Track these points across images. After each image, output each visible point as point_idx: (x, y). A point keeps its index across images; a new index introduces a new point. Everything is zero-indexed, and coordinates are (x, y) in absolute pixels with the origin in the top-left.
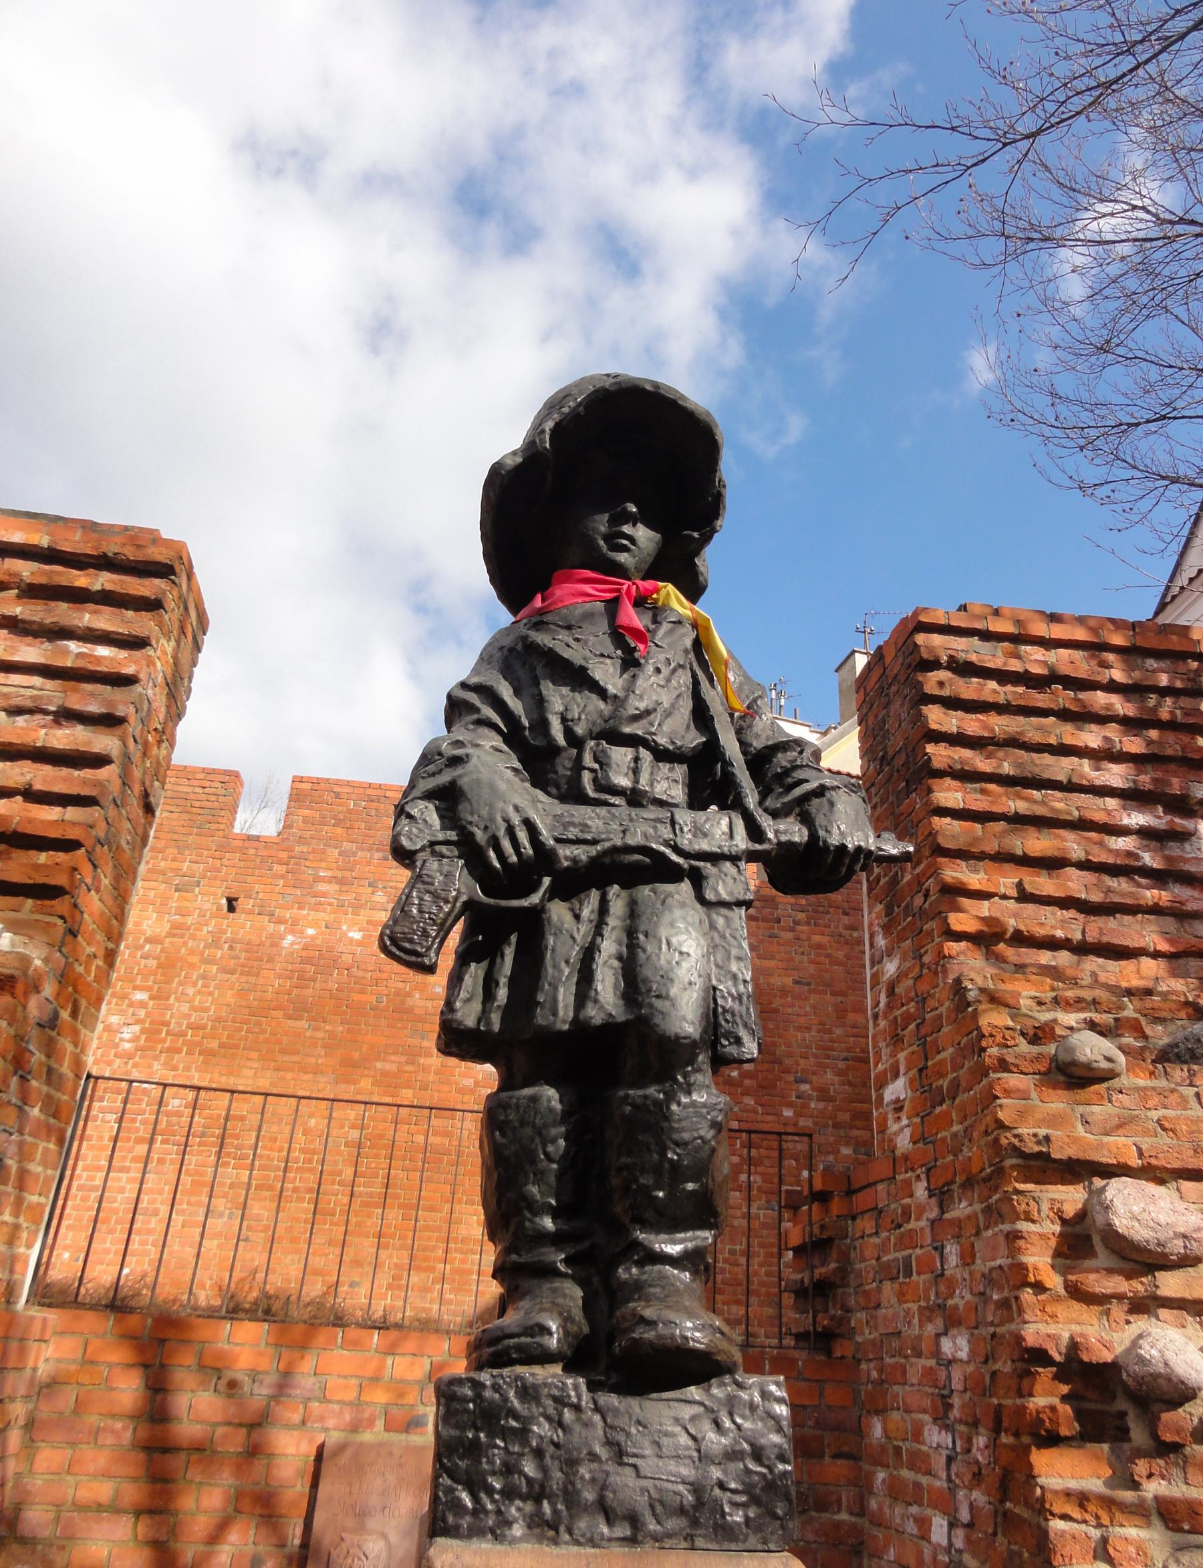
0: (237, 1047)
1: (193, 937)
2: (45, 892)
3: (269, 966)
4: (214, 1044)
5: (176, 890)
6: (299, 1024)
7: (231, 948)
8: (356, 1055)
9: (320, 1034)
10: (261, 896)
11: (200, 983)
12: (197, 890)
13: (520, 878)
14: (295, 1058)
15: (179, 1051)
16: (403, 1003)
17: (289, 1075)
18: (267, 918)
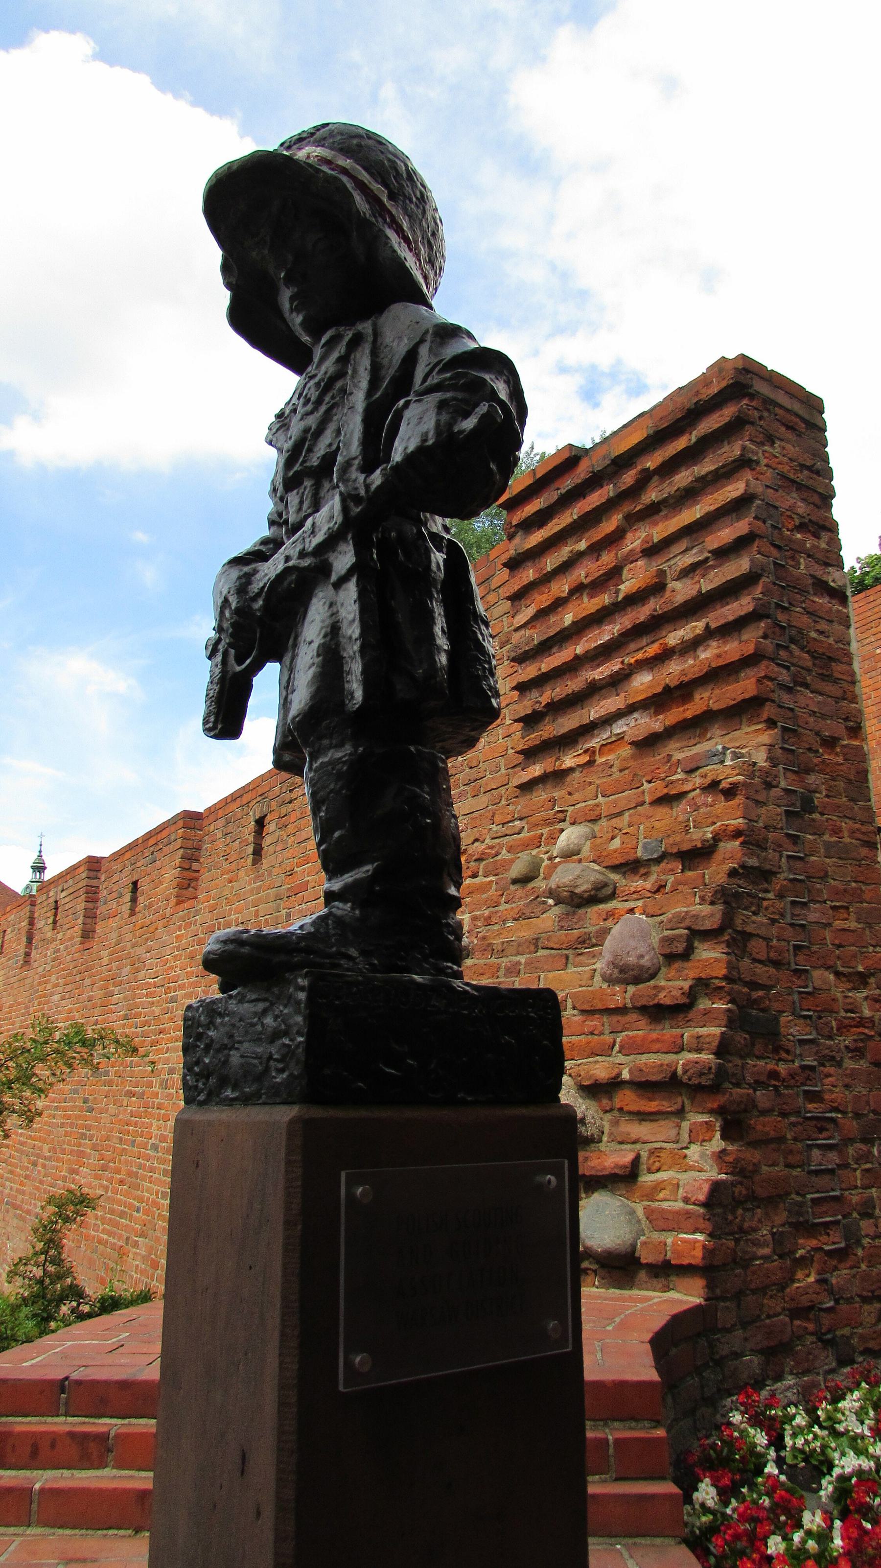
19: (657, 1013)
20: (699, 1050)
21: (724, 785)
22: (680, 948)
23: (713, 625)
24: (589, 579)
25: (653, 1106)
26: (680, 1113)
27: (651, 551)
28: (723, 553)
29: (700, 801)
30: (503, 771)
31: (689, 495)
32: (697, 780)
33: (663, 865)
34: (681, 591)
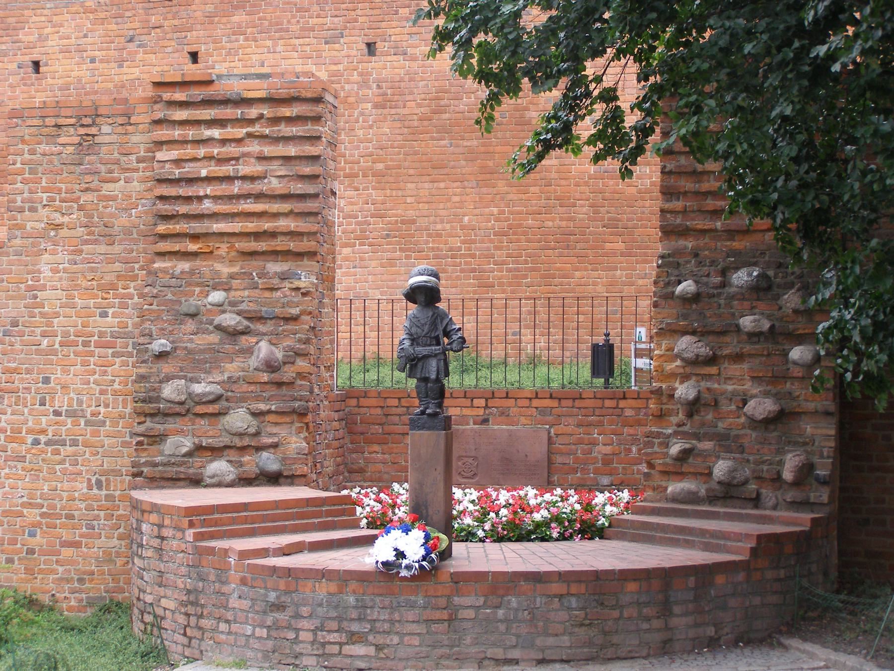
0: (399, 167)
1: (348, 82)
2: (312, 254)
3: (410, 97)
4: (380, 166)
5: (326, 43)
6: (443, 142)
7: (379, 87)
8: (490, 163)
9: (460, 150)
10: (393, 38)
11: (361, 120)
12: (342, 40)
13: (413, 360)
14: (446, 171)
15: (357, 176)
16: (522, 117)
17: (442, 185)
18: (401, 58)
19: (280, 384)
20: (300, 400)
21: (302, 291)
22: (292, 360)
23: (296, 211)
24: (220, 157)
25: (283, 420)
26: (292, 423)
27: (262, 158)
28: (303, 178)
29: (288, 293)
30: (135, 236)
31: (287, 139)
32: (287, 284)
33: (274, 321)
34: (274, 185)
